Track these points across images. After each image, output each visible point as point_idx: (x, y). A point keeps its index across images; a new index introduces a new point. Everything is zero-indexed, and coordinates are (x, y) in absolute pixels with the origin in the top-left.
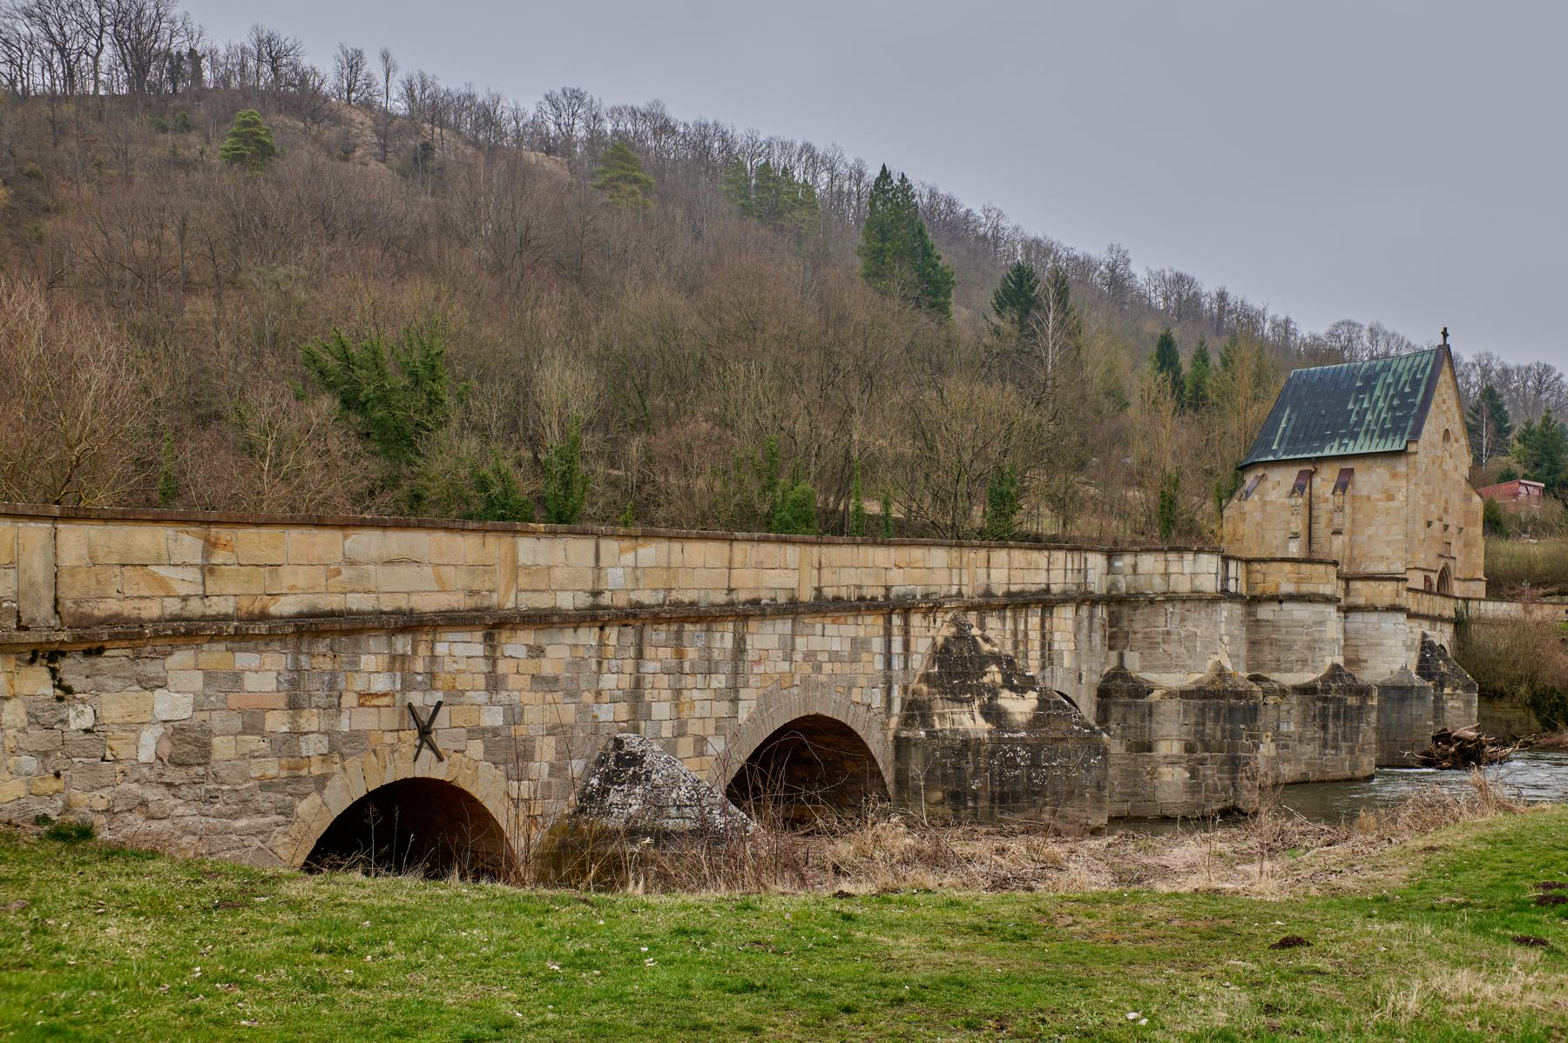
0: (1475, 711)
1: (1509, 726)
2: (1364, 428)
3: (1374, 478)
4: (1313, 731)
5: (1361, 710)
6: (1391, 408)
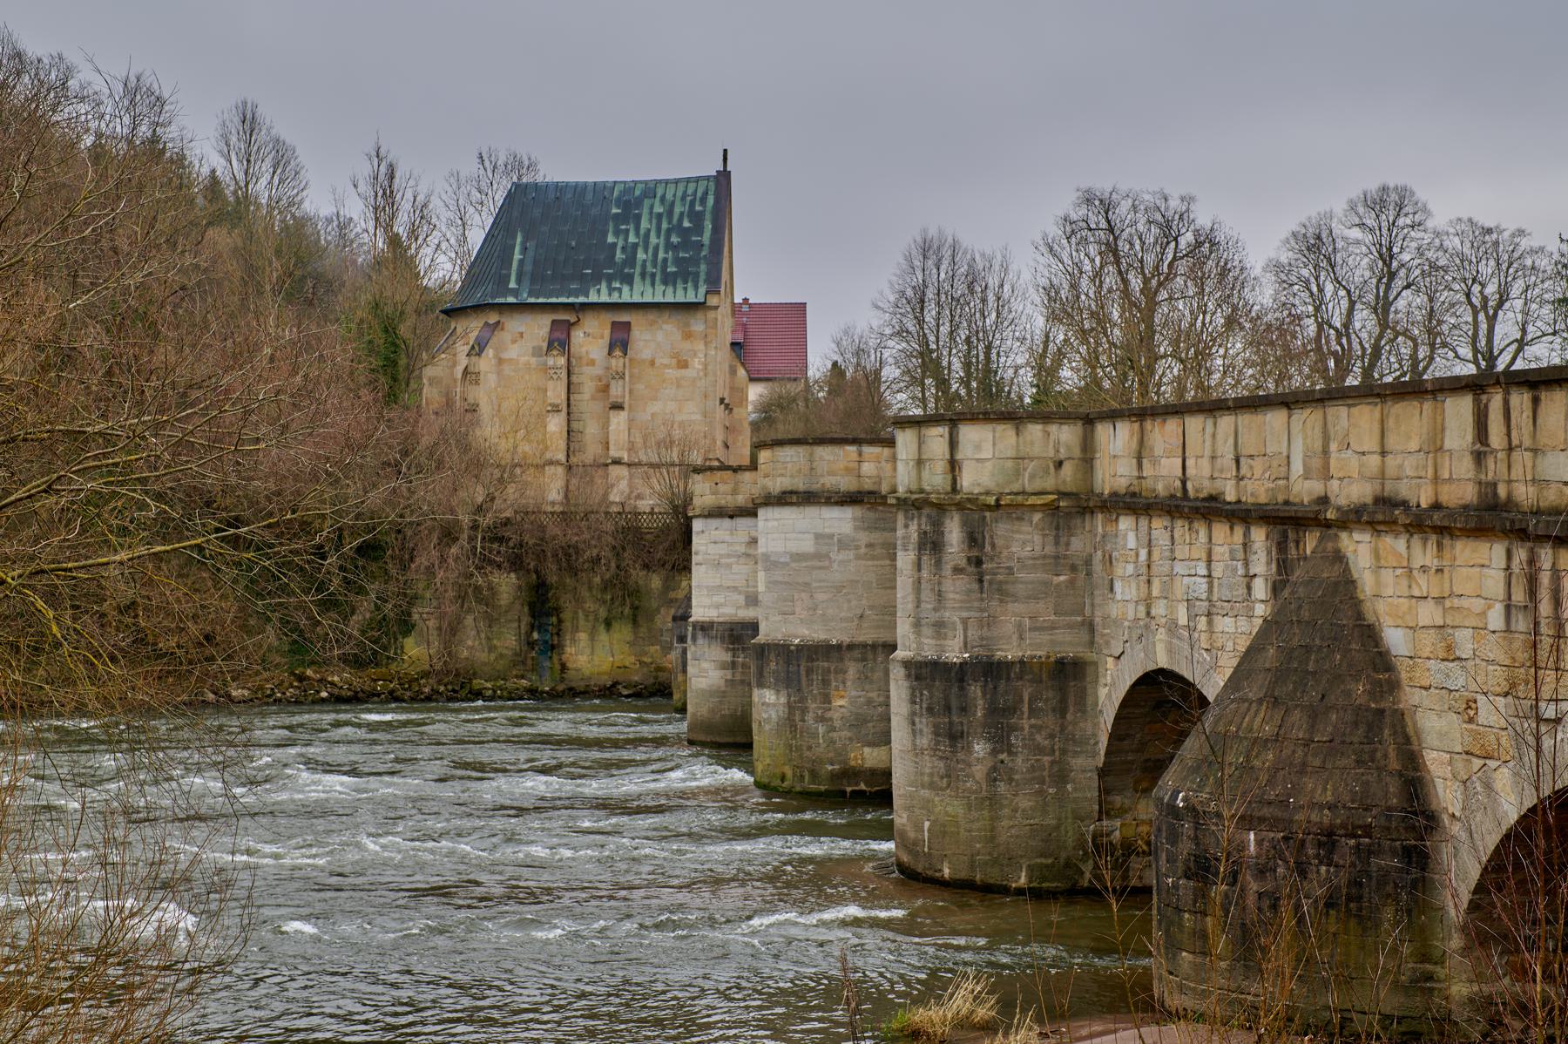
2: (638, 270)
3: (660, 336)
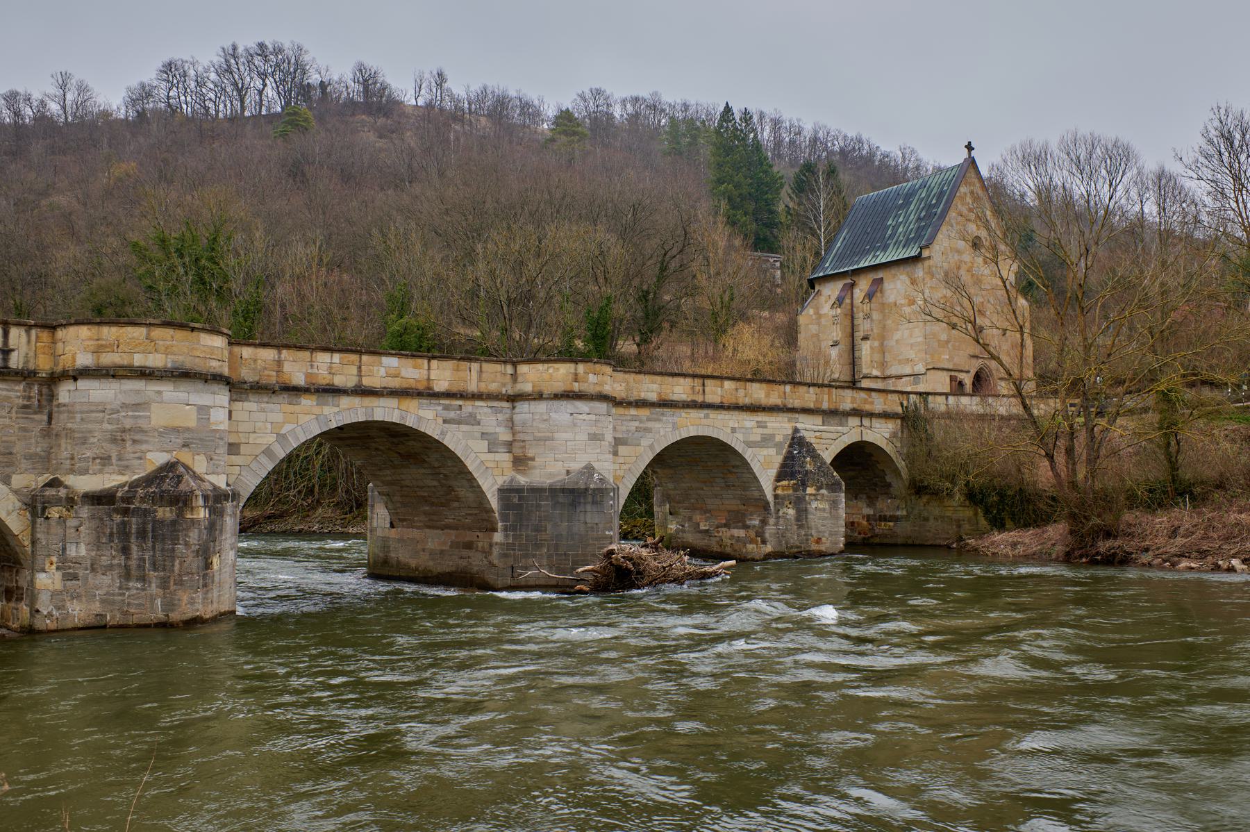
0: (842, 513)
1: (959, 526)
3: (899, 284)
5: (175, 528)
6: (919, 219)
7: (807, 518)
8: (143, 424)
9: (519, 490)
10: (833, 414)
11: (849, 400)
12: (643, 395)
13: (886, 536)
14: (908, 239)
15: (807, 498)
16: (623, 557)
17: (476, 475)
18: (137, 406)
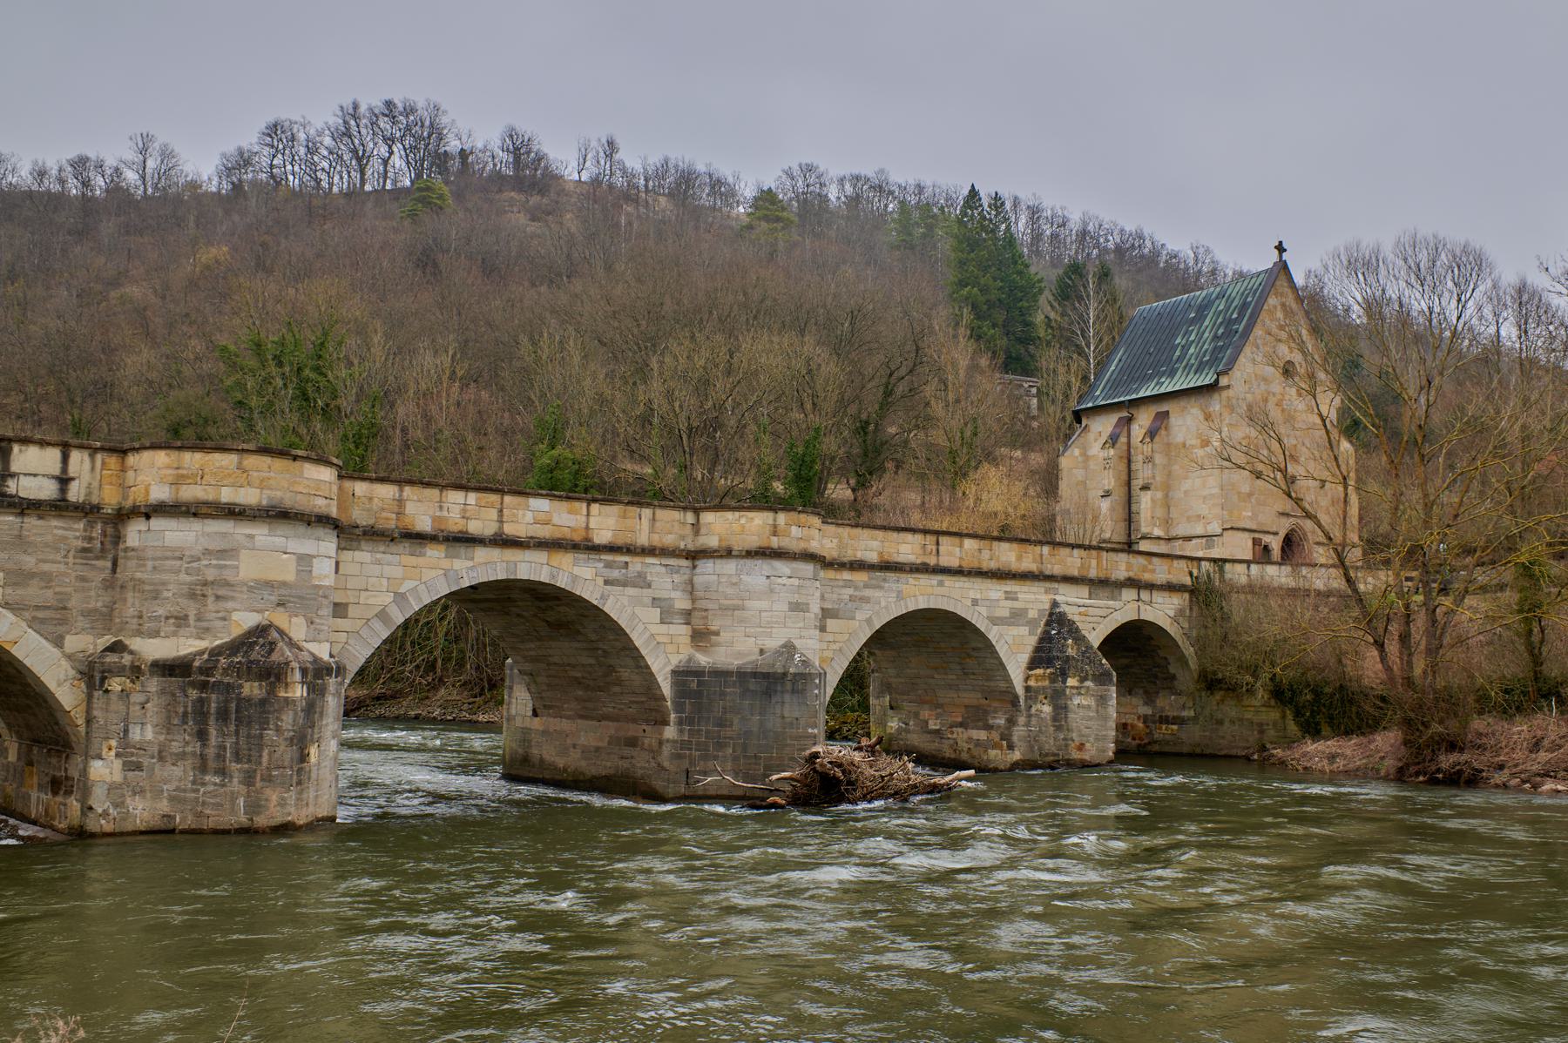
1: (1262, 732)
3: (1189, 420)
4: (183, 741)
5: (266, 708)
6: (1216, 338)
7: (1066, 718)
8: (228, 575)
9: (698, 673)
10: (1102, 585)
11: (1123, 567)
12: (860, 555)
13: (1167, 743)
14: (1201, 363)
15: (1068, 691)
16: (830, 763)
17: (643, 652)
18: (222, 553)
